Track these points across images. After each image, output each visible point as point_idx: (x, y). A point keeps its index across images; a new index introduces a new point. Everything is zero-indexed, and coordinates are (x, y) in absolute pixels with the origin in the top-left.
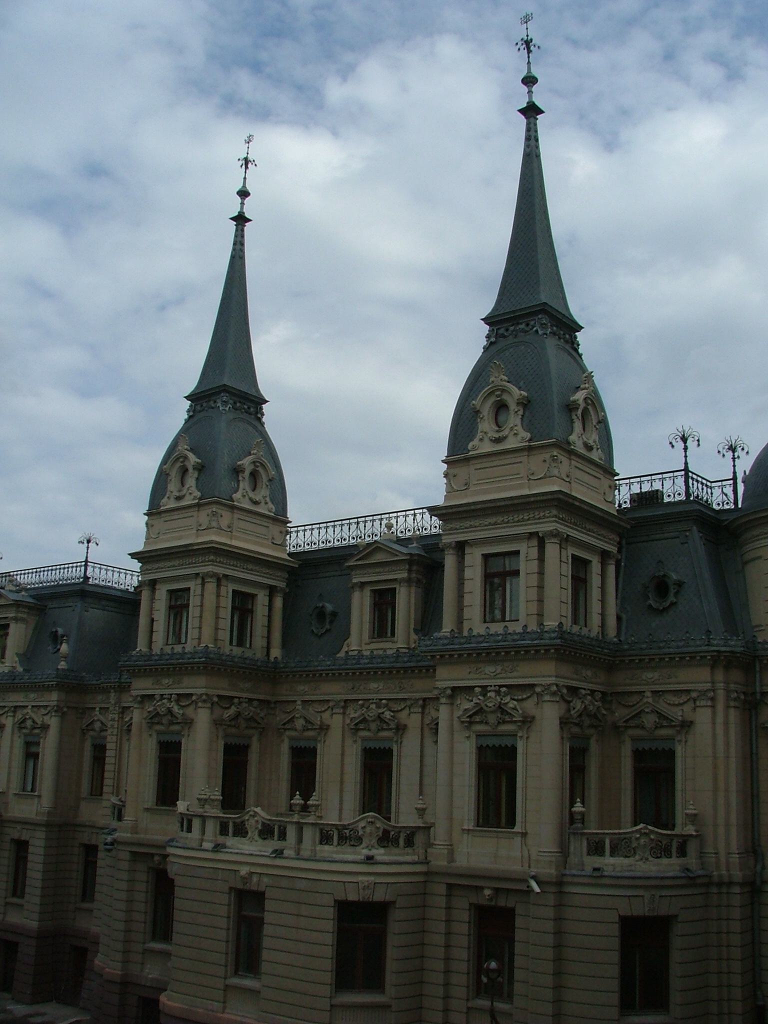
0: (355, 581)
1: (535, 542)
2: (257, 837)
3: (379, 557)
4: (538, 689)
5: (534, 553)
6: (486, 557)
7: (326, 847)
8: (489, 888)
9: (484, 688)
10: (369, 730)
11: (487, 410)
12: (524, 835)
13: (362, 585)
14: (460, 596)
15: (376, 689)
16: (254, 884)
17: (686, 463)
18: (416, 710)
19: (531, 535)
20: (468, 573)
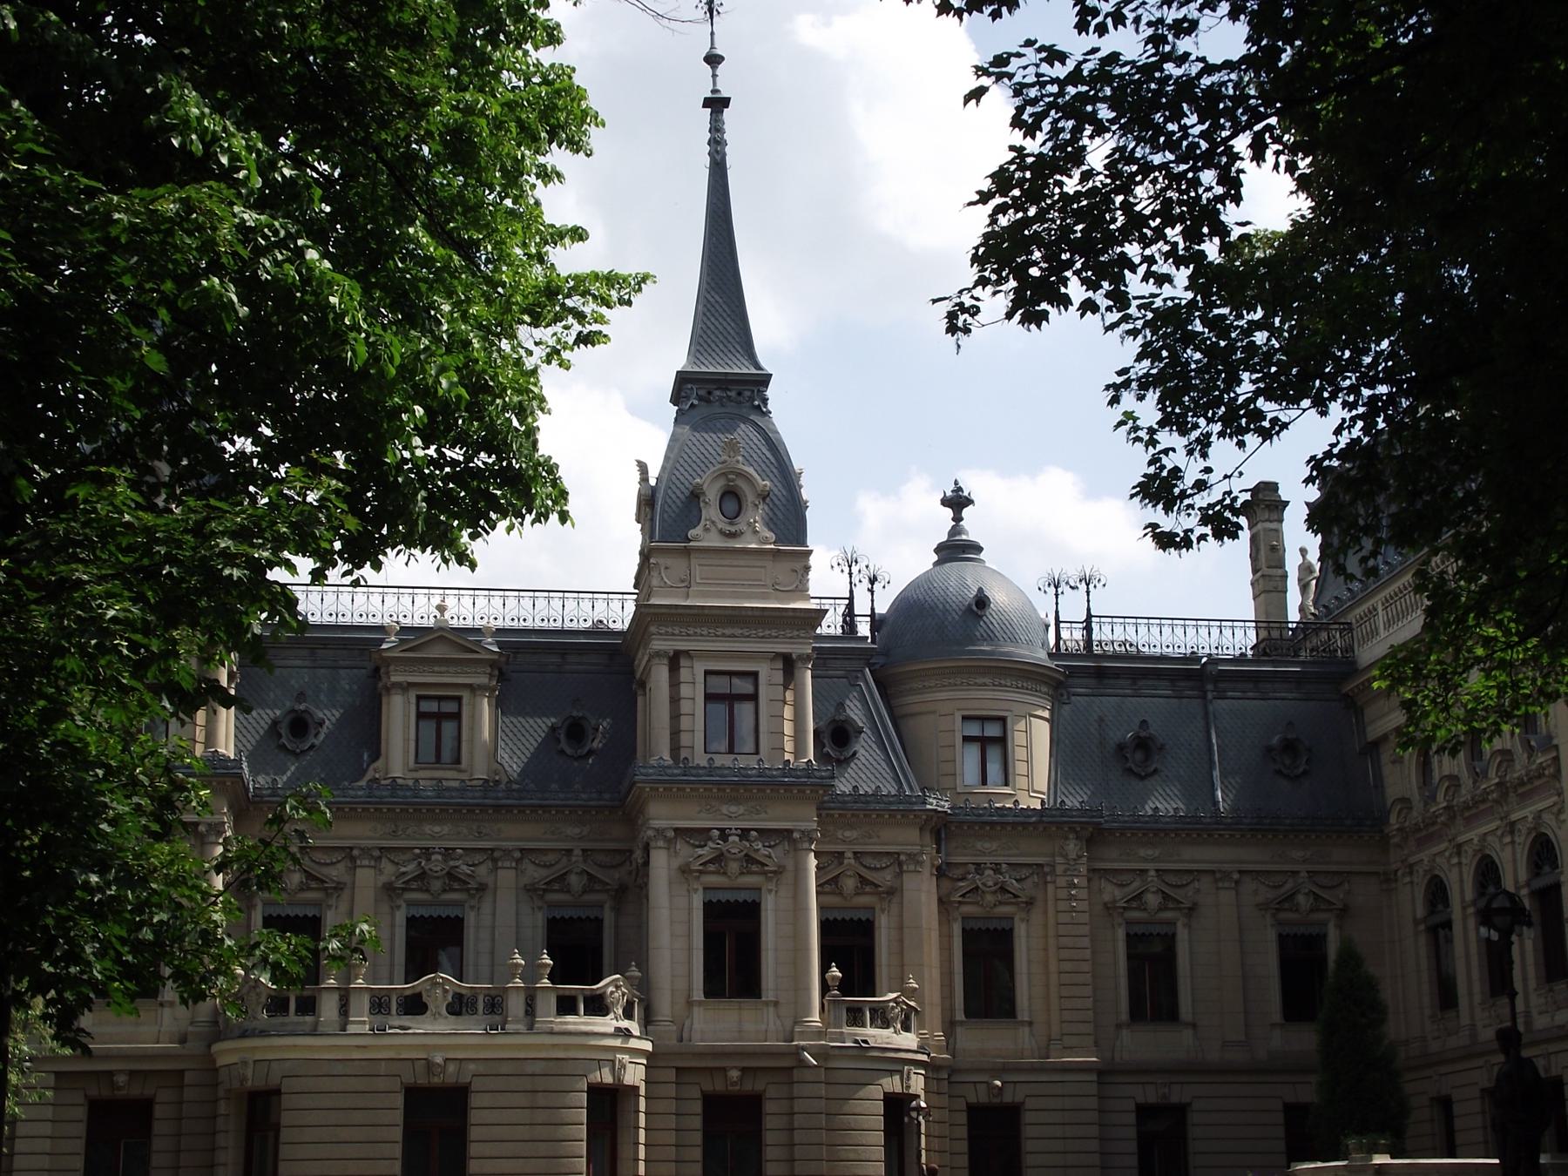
0: (393, 679)
1: (780, 665)
2: (444, 1012)
3: (436, 652)
4: (796, 835)
5: (779, 677)
6: (707, 673)
7: (570, 1018)
8: (736, 1067)
9: (722, 830)
10: (427, 891)
11: (712, 494)
12: (776, 1004)
13: (411, 685)
14: (675, 716)
15: (438, 834)
16: (451, 1075)
17: (851, 592)
18: (507, 864)
19: (778, 655)
20: (685, 691)
